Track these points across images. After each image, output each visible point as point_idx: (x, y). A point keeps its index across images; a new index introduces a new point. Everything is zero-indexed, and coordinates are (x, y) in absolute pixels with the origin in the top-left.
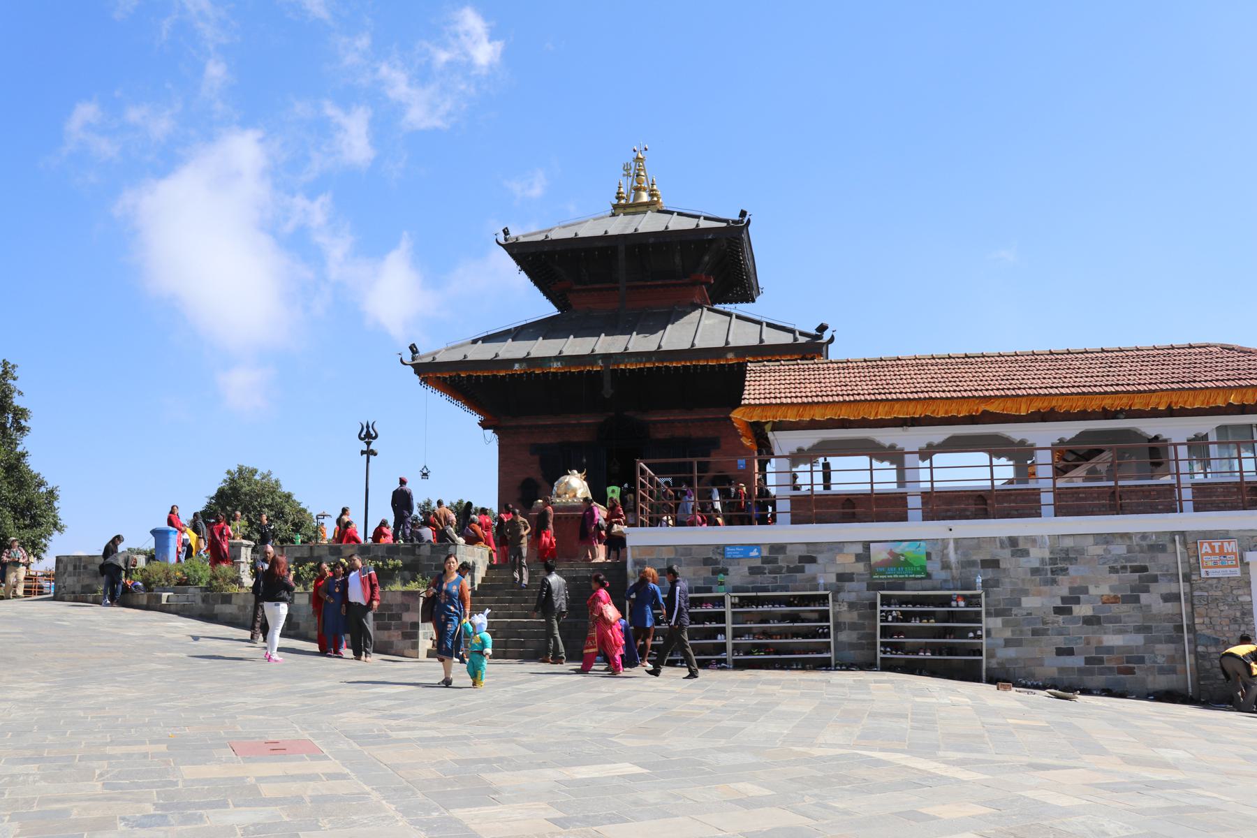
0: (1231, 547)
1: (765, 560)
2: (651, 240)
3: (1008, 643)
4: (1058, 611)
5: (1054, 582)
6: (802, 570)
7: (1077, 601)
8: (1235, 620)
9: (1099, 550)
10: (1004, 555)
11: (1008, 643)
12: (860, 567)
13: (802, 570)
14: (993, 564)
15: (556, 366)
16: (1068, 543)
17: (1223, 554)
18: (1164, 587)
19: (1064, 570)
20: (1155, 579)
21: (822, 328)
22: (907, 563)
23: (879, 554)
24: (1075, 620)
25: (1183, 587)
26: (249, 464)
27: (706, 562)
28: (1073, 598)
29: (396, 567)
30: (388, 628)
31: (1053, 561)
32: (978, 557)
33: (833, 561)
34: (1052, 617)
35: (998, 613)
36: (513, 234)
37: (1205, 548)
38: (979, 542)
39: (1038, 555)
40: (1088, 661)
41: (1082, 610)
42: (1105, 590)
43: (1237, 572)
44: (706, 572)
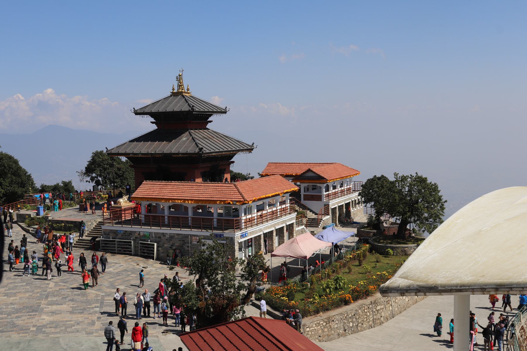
3: (162, 253)
9: (176, 236)
11: (162, 253)
14: (160, 237)
18: (187, 245)
19: (171, 240)
22: (146, 236)
23: (142, 234)
27: (115, 233)
36: (136, 109)
39: (167, 236)
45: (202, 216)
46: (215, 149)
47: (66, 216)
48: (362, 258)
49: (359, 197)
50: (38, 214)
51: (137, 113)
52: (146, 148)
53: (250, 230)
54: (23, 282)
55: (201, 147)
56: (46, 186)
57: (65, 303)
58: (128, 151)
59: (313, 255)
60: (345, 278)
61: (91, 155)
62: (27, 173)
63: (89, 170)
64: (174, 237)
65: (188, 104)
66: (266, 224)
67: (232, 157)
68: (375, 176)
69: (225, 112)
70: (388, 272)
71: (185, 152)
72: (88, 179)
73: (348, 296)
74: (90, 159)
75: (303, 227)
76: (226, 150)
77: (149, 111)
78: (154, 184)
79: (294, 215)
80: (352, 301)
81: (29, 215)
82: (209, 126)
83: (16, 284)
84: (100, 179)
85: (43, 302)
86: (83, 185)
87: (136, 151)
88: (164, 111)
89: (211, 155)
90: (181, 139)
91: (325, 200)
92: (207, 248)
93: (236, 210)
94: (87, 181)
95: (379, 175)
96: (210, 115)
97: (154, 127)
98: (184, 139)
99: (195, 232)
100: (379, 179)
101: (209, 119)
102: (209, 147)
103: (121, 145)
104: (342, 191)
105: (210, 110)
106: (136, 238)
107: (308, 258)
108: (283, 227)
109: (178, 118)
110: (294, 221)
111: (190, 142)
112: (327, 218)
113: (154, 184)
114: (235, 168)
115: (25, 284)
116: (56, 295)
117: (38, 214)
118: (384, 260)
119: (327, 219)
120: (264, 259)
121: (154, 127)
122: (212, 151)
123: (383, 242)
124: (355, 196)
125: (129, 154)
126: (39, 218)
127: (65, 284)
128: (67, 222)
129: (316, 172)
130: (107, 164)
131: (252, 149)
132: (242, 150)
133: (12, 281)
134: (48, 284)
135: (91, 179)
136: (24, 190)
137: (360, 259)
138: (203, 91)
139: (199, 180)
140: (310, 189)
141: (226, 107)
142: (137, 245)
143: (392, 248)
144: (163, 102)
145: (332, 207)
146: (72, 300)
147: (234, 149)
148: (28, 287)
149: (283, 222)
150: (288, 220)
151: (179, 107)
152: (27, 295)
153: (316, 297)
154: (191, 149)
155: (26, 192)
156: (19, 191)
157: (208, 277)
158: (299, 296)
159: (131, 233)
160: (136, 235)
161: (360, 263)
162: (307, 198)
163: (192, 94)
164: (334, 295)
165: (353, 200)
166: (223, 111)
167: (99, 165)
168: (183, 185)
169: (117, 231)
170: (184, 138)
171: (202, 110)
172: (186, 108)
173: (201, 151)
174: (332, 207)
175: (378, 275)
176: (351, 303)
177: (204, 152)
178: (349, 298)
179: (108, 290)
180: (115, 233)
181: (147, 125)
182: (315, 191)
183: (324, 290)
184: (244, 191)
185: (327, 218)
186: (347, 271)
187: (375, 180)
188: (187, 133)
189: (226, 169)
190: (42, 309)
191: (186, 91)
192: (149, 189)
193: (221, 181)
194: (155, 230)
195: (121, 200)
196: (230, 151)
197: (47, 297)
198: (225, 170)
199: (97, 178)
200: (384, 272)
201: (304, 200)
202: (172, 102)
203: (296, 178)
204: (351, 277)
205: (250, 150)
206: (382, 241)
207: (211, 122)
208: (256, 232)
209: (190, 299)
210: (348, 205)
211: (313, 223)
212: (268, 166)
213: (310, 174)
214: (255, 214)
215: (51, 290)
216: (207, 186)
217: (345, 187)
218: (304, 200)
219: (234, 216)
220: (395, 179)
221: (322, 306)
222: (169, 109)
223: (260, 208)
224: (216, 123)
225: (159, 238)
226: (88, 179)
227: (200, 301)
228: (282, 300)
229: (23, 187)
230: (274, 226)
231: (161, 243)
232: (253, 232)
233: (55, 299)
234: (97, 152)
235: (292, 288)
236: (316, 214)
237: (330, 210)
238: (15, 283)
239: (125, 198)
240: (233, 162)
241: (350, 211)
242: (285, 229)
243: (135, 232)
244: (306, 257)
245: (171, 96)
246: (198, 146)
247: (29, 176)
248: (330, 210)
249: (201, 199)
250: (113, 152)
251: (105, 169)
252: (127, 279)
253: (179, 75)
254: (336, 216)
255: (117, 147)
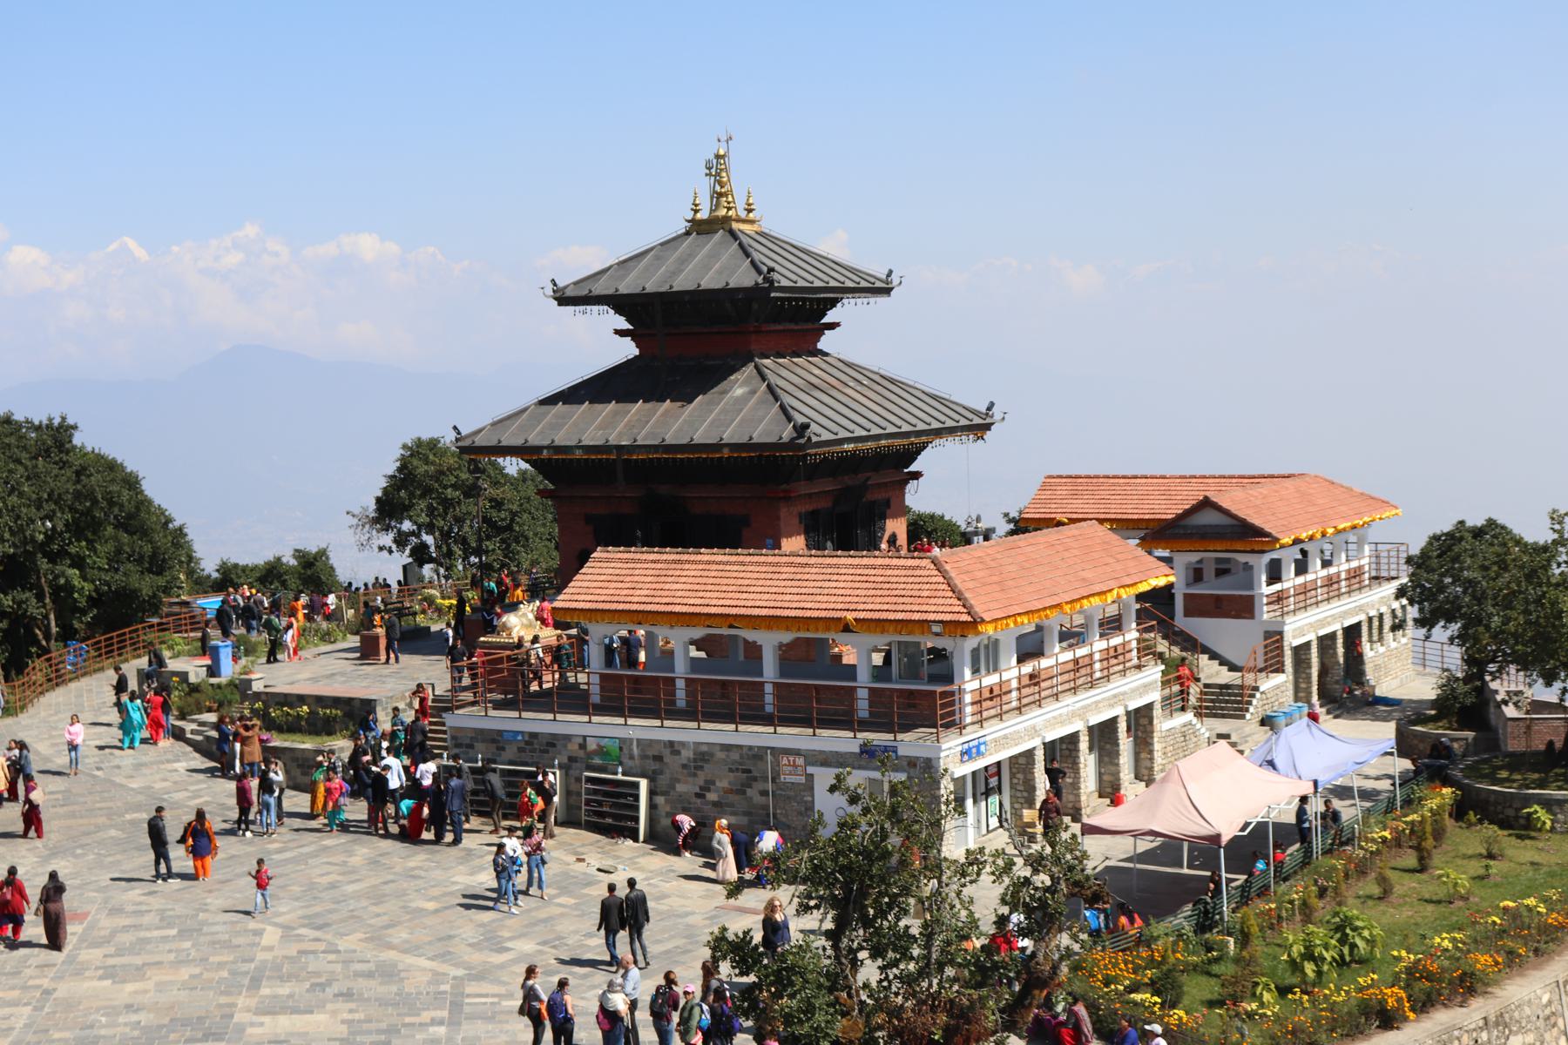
0: (800, 761)
1: (527, 743)
2: (687, 298)
4: (698, 795)
5: (695, 775)
7: (709, 790)
8: (800, 814)
9: (721, 755)
10: (666, 753)
12: (581, 754)
15: (578, 454)
16: (705, 748)
17: (795, 766)
18: (759, 786)
19: (701, 768)
20: (755, 779)
24: (708, 803)
25: (770, 787)
28: (706, 787)
31: (695, 760)
32: (650, 753)
33: (565, 746)
34: (694, 799)
35: (663, 794)
36: (561, 284)
37: (785, 761)
39: (687, 754)
41: (712, 796)
42: (723, 784)
43: (802, 779)
45: (810, 680)
46: (851, 426)
47: (314, 680)
48: (1429, 843)
49: (1396, 605)
50: (213, 671)
51: (563, 299)
52: (600, 428)
53: (993, 730)
54: (170, 926)
55: (800, 419)
56: (236, 566)
57: (321, 1006)
58: (534, 439)
59: (1243, 829)
60: (1371, 922)
61: (398, 452)
62: (169, 520)
63: (388, 509)
64: (712, 755)
65: (753, 263)
66: (1051, 709)
67: (912, 454)
68: (1462, 523)
69: (887, 291)
70: (1545, 900)
71: (744, 440)
72: (387, 539)
73: (1393, 996)
74: (391, 467)
75: (1189, 716)
76: (891, 429)
77: (611, 291)
78: (633, 561)
79: (1155, 672)
80: (1412, 1016)
81: (184, 676)
82: (826, 342)
83: (143, 934)
84: (429, 539)
85: (241, 1001)
86: (369, 562)
87: (562, 439)
88: (665, 289)
89: (837, 449)
90: (725, 392)
91: (1266, 614)
92: (866, 811)
93: (939, 655)
94: (381, 549)
95: (1476, 520)
96: (833, 303)
97: (628, 349)
98: (739, 392)
99: (791, 737)
100: (1478, 533)
101: (830, 317)
102: (835, 422)
103: (509, 417)
104: (1330, 582)
105: (833, 284)
106: (571, 759)
107: (1225, 840)
108: (1114, 720)
109: (714, 317)
110: (1155, 696)
111: (761, 402)
112: (1276, 687)
113: (633, 561)
114: (919, 498)
115: (174, 932)
116: (289, 977)
117: (213, 671)
118: (1519, 852)
119: (1278, 687)
120: (1085, 855)
121: (628, 349)
122: (843, 434)
123: (1507, 780)
124: (1380, 599)
125: (539, 449)
126: (219, 686)
127: (317, 934)
128: (320, 700)
129: (1234, 509)
130: (455, 487)
131: (988, 427)
132: (952, 431)
133: (127, 922)
134: (258, 933)
135: (395, 541)
136: (161, 581)
137: (1420, 846)
138: (804, 217)
139: (794, 543)
140: (1209, 573)
141: (890, 272)
142: (574, 787)
143: (1548, 804)
144: (657, 258)
145: (1292, 640)
146: (347, 995)
147: (921, 426)
148: (187, 944)
149: (1116, 699)
150: (1133, 691)
151: (720, 272)
152: (185, 973)
153: (1267, 997)
154: (766, 428)
155: (167, 590)
156: (145, 585)
157: (867, 923)
158: (1197, 988)
159: (552, 743)
160: (573, 747)
161: (1421, 859)
162: (1197, 607)
163: (766, 226)
164: (1338, 989)
165: (1373, 613)
166: (878, 284)
167: (427, 491)
168: (743, 564)
169: (500, 732)
170: (740, 386)
171: (801, 283)
172: (744, 277)
173: (801, 435)
174: (1292, 640)
175: (1506, 909)
176: (1406, 1019)
177: (814, 439)
178: (1399, 1000)
179: (476, 957)
180: (494, 741)
181: (604, 342)
182: (1226, 579)
183: (1295, 966)
184: (971, 585)
185: (1276, 687)
186: (1376, 890)
187: (1461, 539)
188: (749, 369)
189: (891, 504)
190: (241, 1029)
191: (743, 214)
192: (616, 578)
193: (872, 545)
194: (641, 729)
195: (511, 619)
196: (907, 435)
197: (255, 983)
198: (887, 503)
199: (418, 536)
200: (1531, 902)
201: (1188, 613)
202: (691, 255)
203: (1158, 534)
204: (1397, 914)
205: (979, 429)
206: (1504, 774)
207: (833, 326)
208: (1017, 738)
209: (809, 1009)
210: (1352, 633)
211: (1226, 703)
212: (1044, 487)
213: (1208, 518)
214: (1011, 671)
215: (268, 956)
216: (830, 566)
217: (1341, 567)
218: (1188, 613)
219: (933, 679)
220: (1551, 537)
221: (1293, 1033)
222: (683, 283)
223: (1030, 649)
224: (852, 333)
225: (655, 760)
226: (387, 539)
227: (844, 1014)
228: (1136, 1004)
229: (159, 573)
230: (1081, 714)
231: (663, 780)
232: (1005, 737)
233: (284, 990)
234: (419, 443)
235: (1172, 960)
236: (1233, 668)
237: (1288, 654)
238: (136, 927)
239: (528, 610)
240: (916, 475)
241: (1361, 655)
242: (1122, 726)
243: (568, 738)
244: (1218, 836)
245: (688, 233)
246: (789, 419)
247: (180, 532)
248: (1288, 654)
249: (808, 614)
250: (480, 441)
251: (447, 504)
252: (542, 914)
253: (718, 157)
254: (1309, 677)
255: (493, 424)
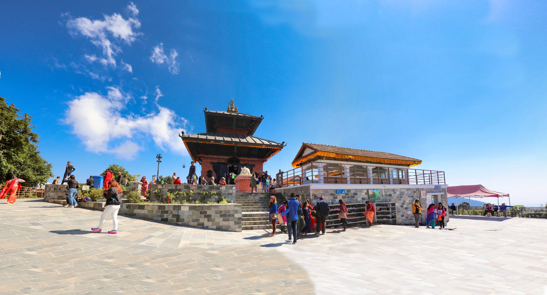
1: (346, 194)
6: (354, 197)
13: (354, 197)
14: (390, 195)
21: (283, 143)
23: (370, 193)
26: (116, 164)
27: (332, 195)
29: (214, 194)
30: (228, 220)
32: (388, 193)
38: (388, 190)
39: (398, 193)
40: (406, 217)
42: (407, 201)
44: (332, 198)
160: (364, 195)
